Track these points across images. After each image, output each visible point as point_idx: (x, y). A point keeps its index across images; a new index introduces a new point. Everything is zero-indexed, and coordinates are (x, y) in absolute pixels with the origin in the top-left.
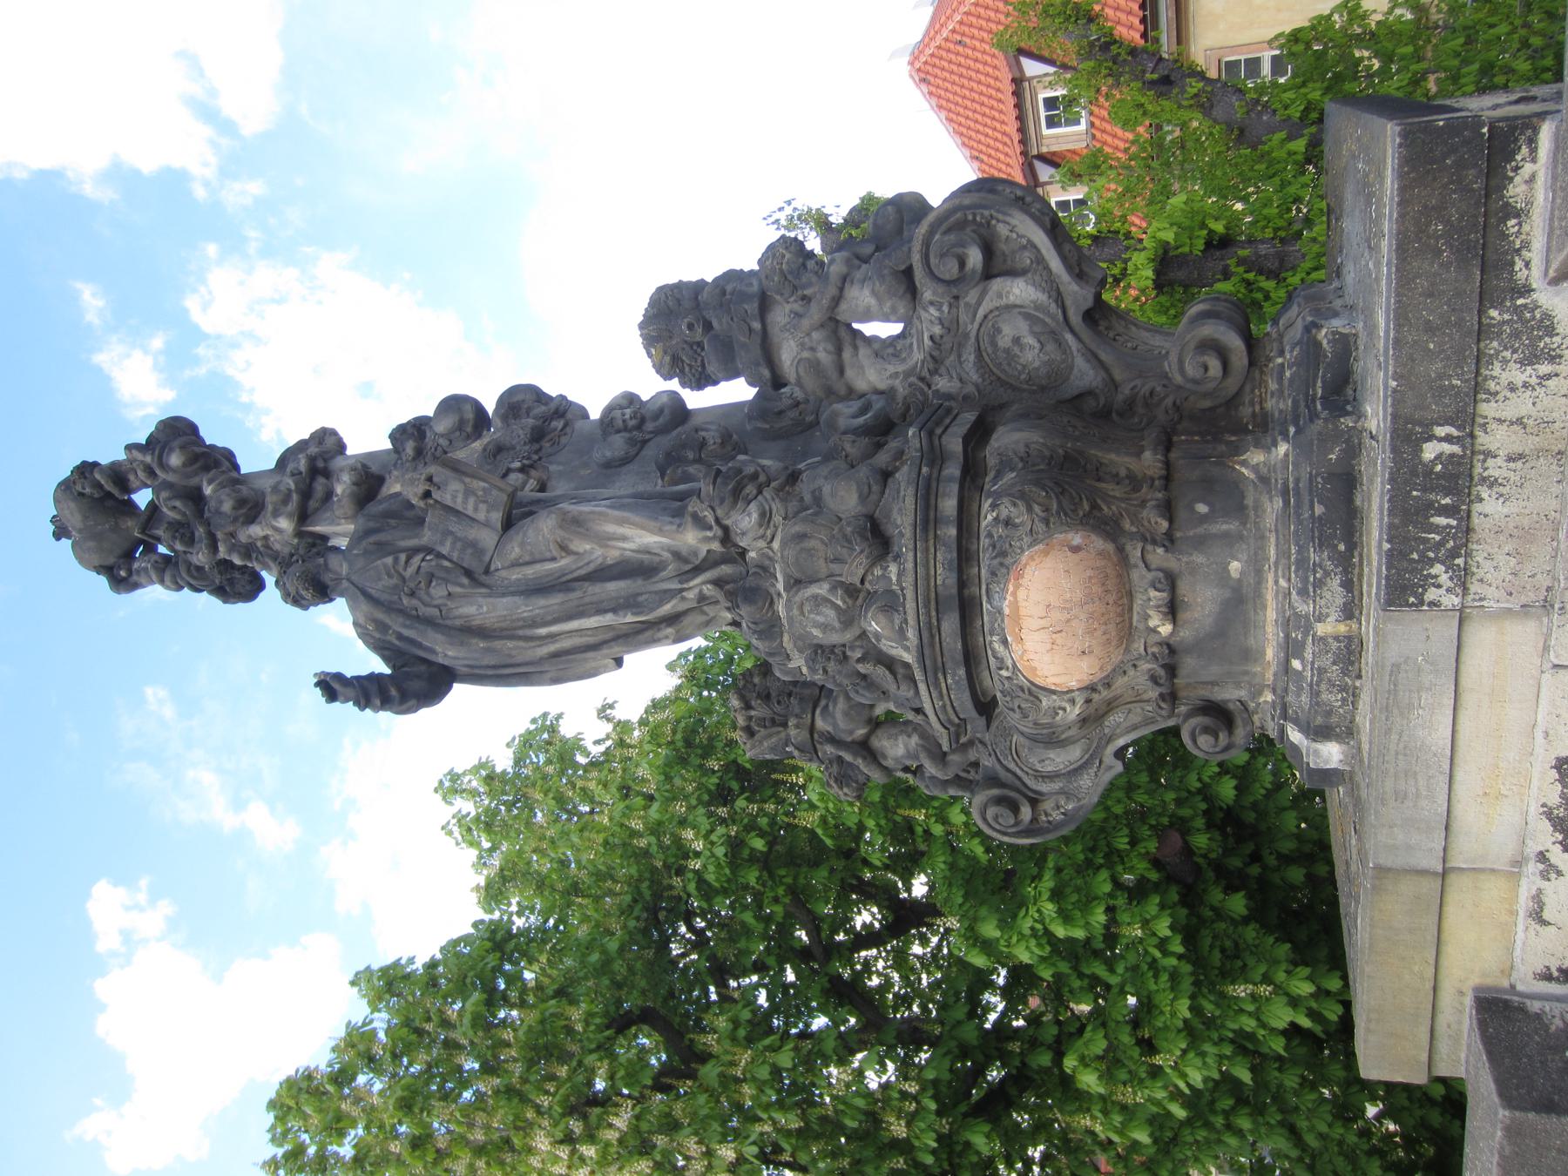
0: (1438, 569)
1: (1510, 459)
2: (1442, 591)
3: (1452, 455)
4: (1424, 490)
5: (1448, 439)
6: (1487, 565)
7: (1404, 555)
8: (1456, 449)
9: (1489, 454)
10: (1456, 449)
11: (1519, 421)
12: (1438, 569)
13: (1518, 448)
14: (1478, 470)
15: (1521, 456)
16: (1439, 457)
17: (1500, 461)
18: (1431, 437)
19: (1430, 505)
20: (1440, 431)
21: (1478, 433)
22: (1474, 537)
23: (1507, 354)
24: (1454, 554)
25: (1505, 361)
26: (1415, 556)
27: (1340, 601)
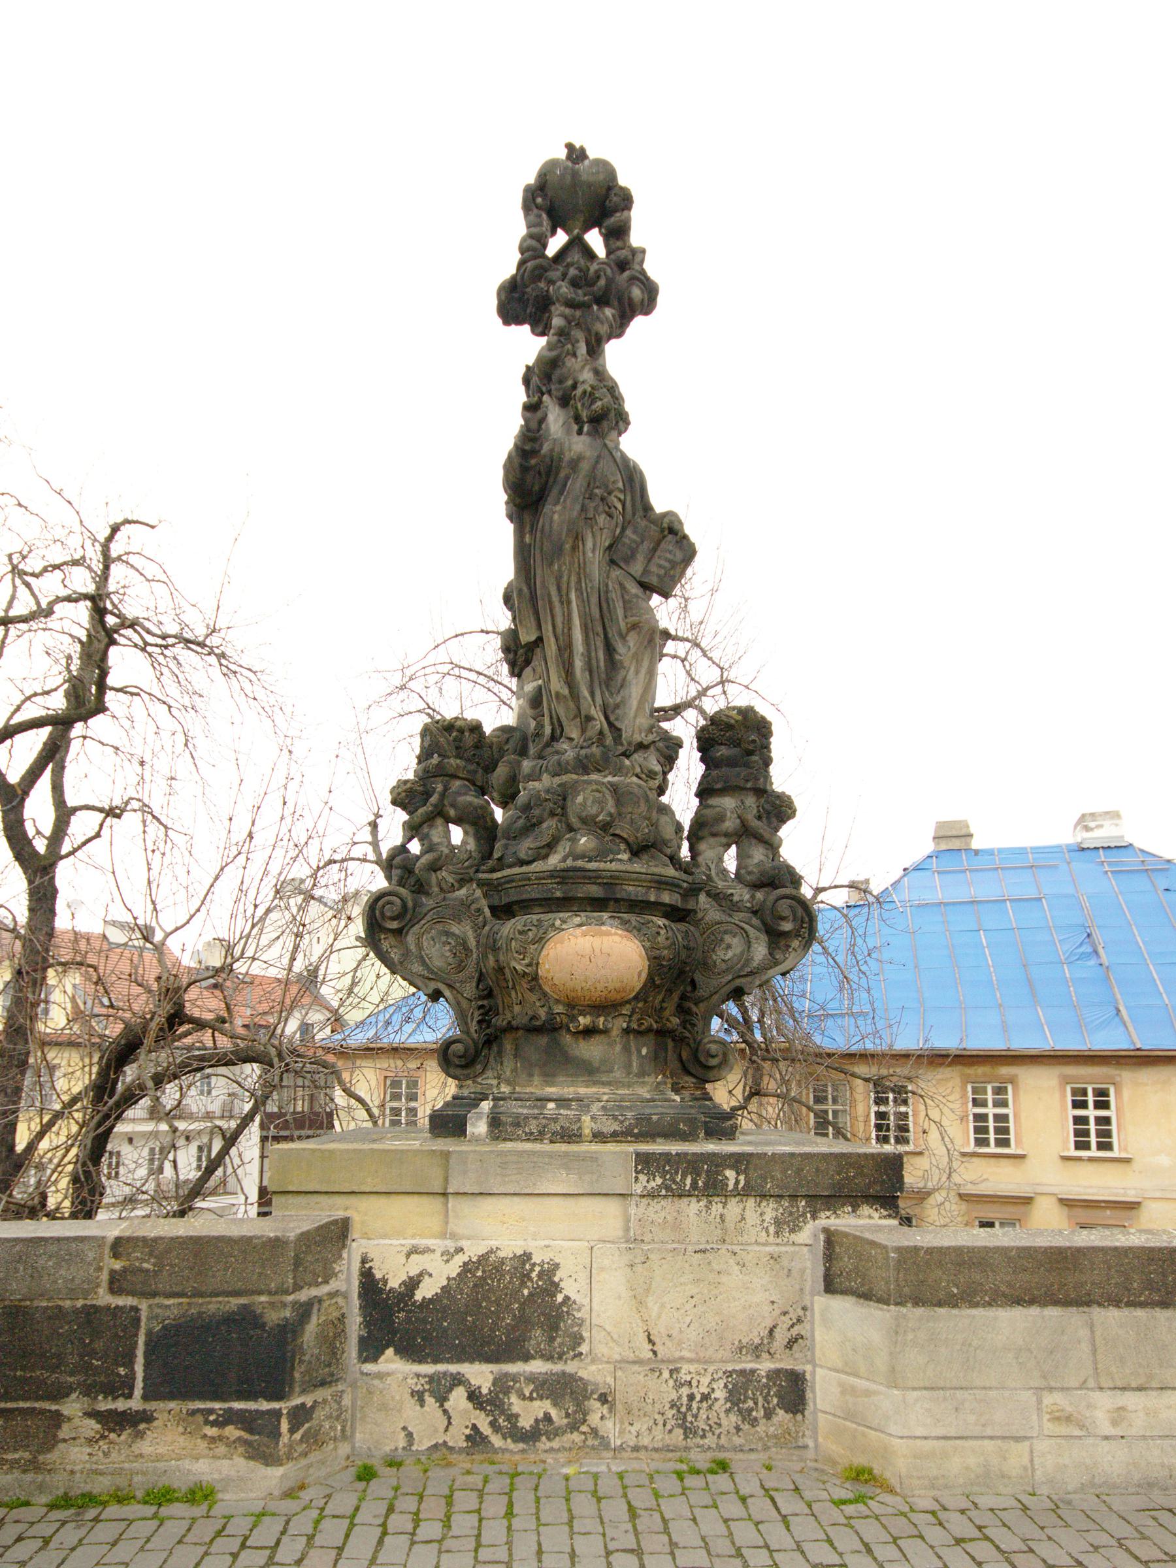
0: (659, 1181)
1: (722, 1216)
2: (645, 1183)
3: (727, 1185)
4: (707, 1171)
5: (737, 1182)
6: (659, 1207)
7: (668, 1162)
8: (731, 1187)
9: (725, 1204)
10: (731, 1187)
11: (743, 1219)
12: (659, 1181)
13: (728, 1219)
14: (716, 1199)
15: (723, 1221)
16: (727, 1178)
17: (721, 1210)
18: (738, 1174)
19: (698, 1175)
20: (742, 1178)
21: (738, 1198)
22: (676, 1199)
23: (781, 1210)
24: (668, 1188)
25: (777, 1210)
26: (667, 1168)
27: (605, 1130)
